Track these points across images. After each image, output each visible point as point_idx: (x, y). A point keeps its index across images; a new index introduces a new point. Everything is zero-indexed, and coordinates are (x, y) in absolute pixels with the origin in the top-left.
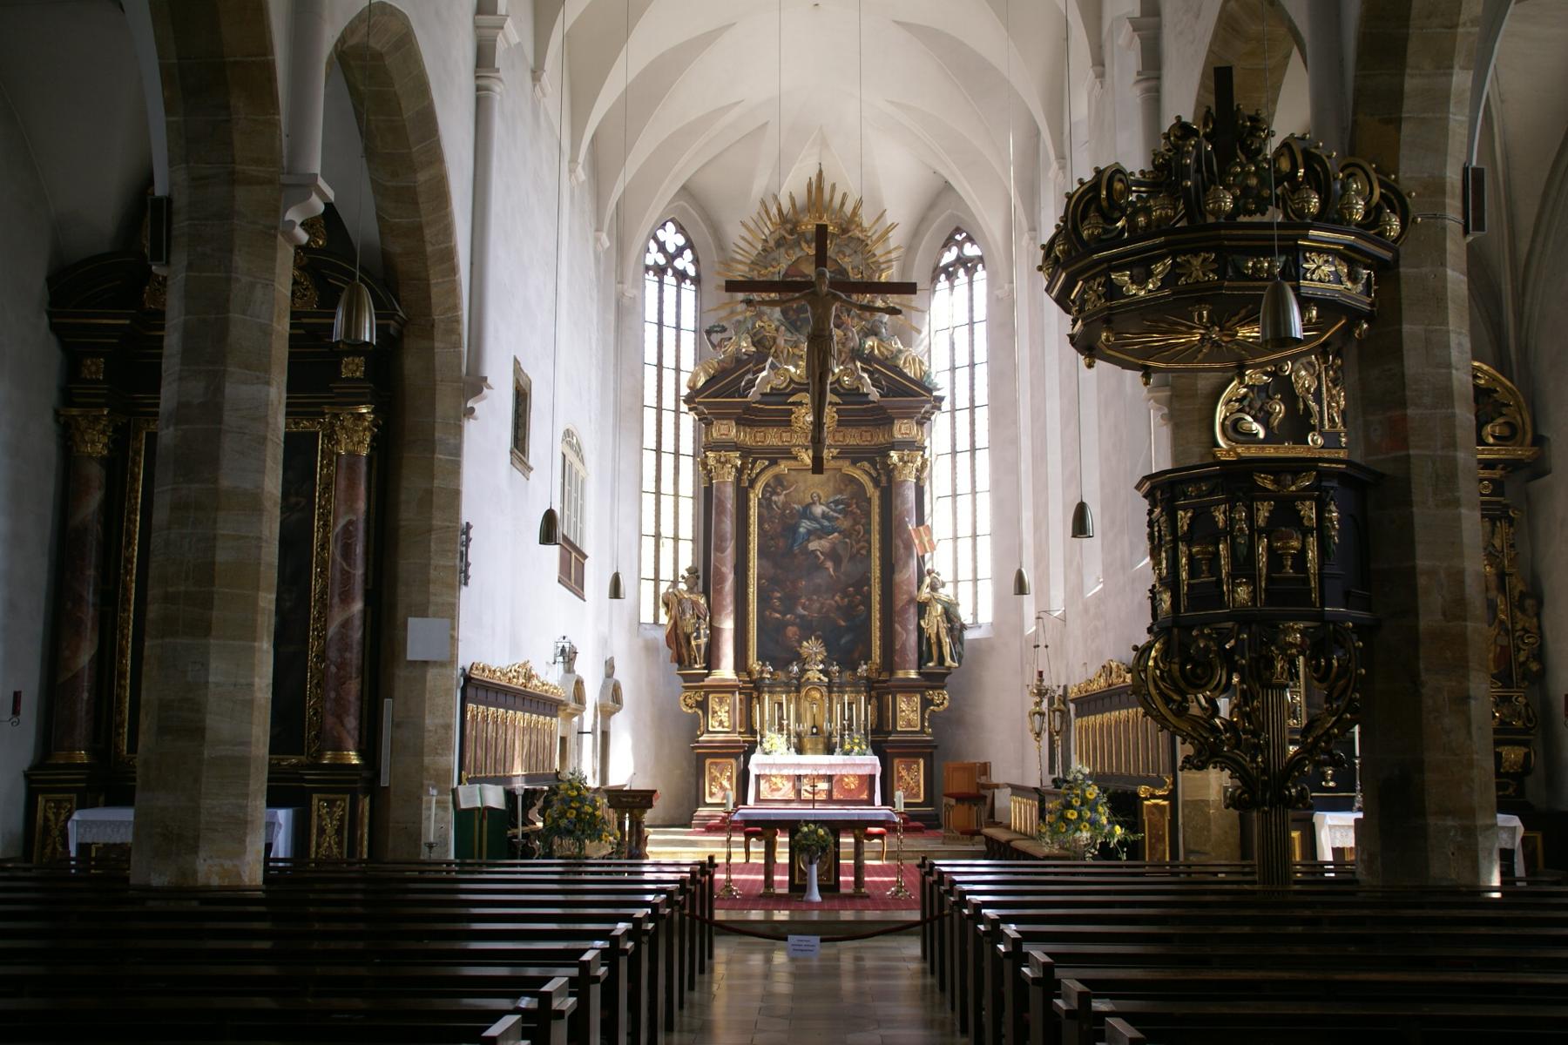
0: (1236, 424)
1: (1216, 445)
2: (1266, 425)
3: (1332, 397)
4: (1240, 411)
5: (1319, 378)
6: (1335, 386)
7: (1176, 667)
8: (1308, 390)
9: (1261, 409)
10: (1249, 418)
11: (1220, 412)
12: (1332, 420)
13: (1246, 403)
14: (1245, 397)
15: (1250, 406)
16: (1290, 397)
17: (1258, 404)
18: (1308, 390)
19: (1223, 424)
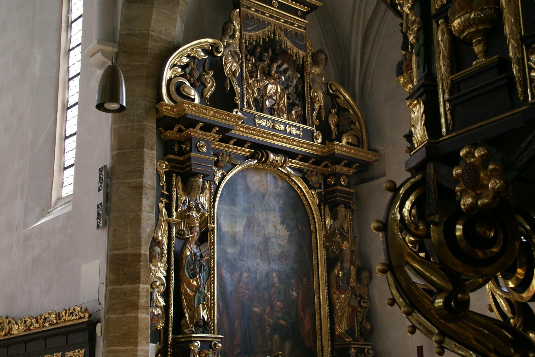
0: (179, 88)
1: (162, 99)
2: (202, 96)
3: (249, 85)
4: (182, 76)
5: (241, 65)
6: (251, 77)
7: (435, 233)
8: (234, 73)
9: (199, 79)
10: (188, 84)
11: (167, 74)
12: (249, 104)
13: (188, 70)
14: (187, 65)
15: (191, 73)
16: (220, 77)
17: (197, 74)
18: (234, 73)
19: (169, 81)
